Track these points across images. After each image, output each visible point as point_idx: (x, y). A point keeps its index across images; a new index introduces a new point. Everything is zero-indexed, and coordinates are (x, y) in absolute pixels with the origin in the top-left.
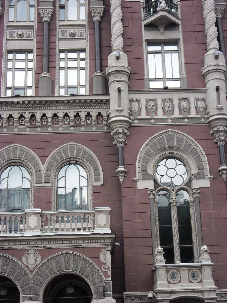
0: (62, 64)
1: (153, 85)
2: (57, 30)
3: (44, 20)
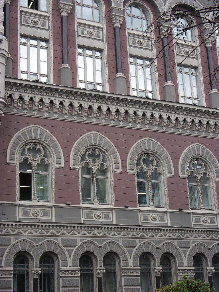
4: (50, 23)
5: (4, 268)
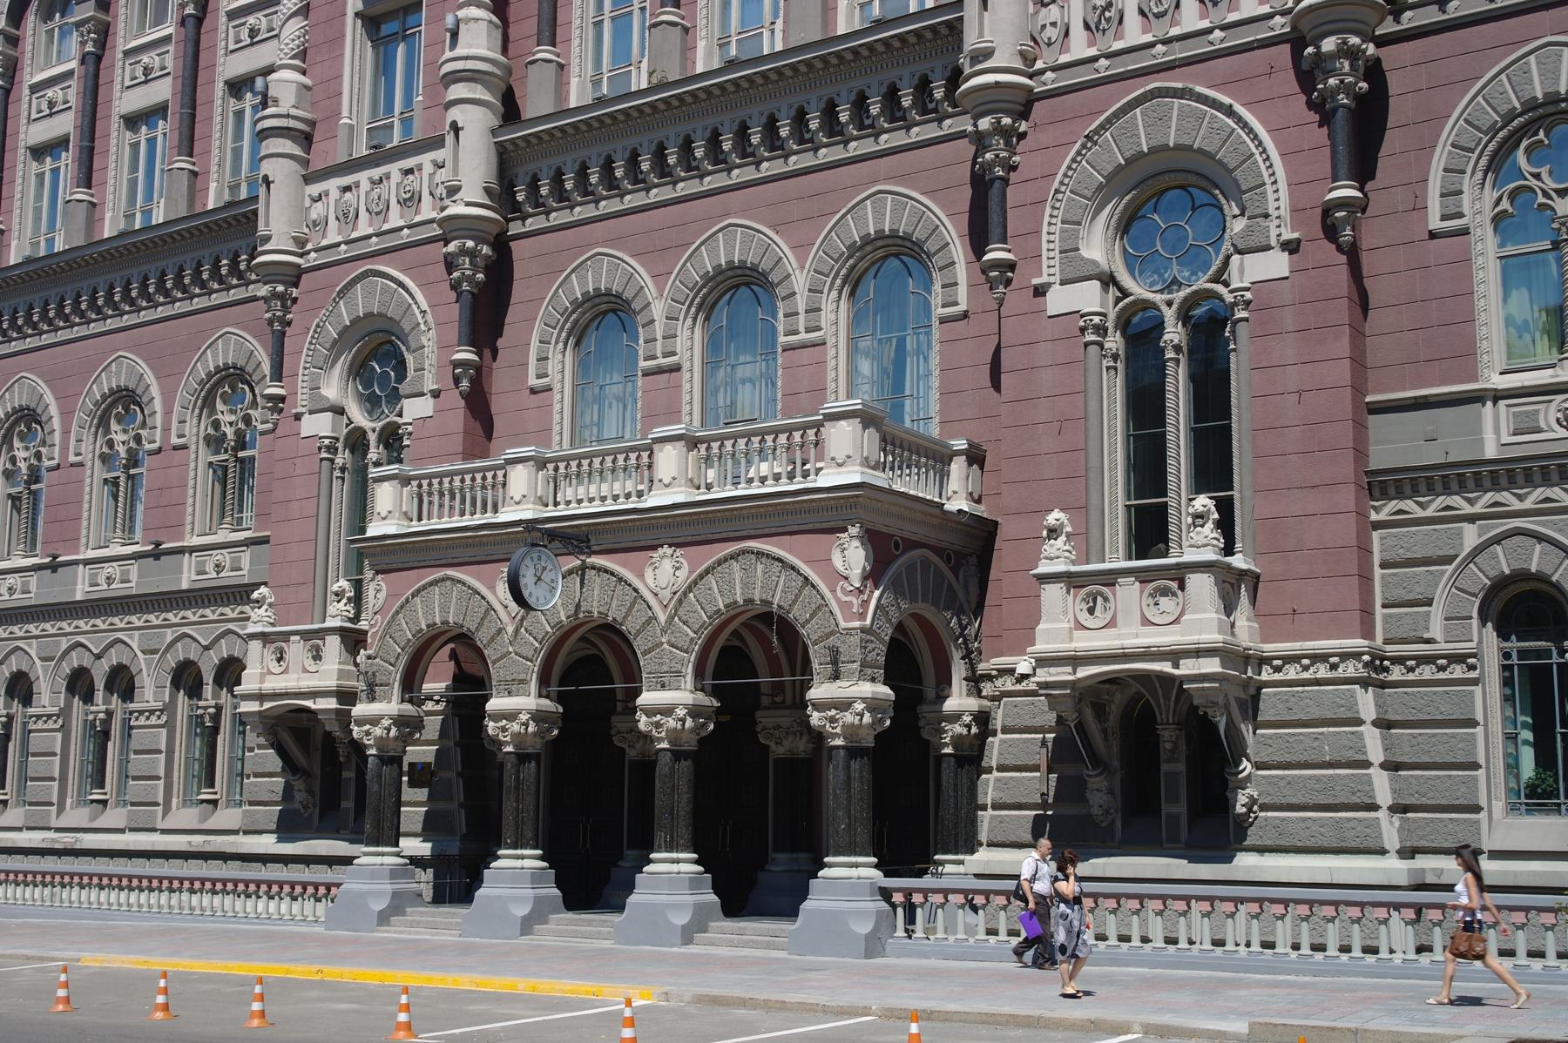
5: (1443, 647)
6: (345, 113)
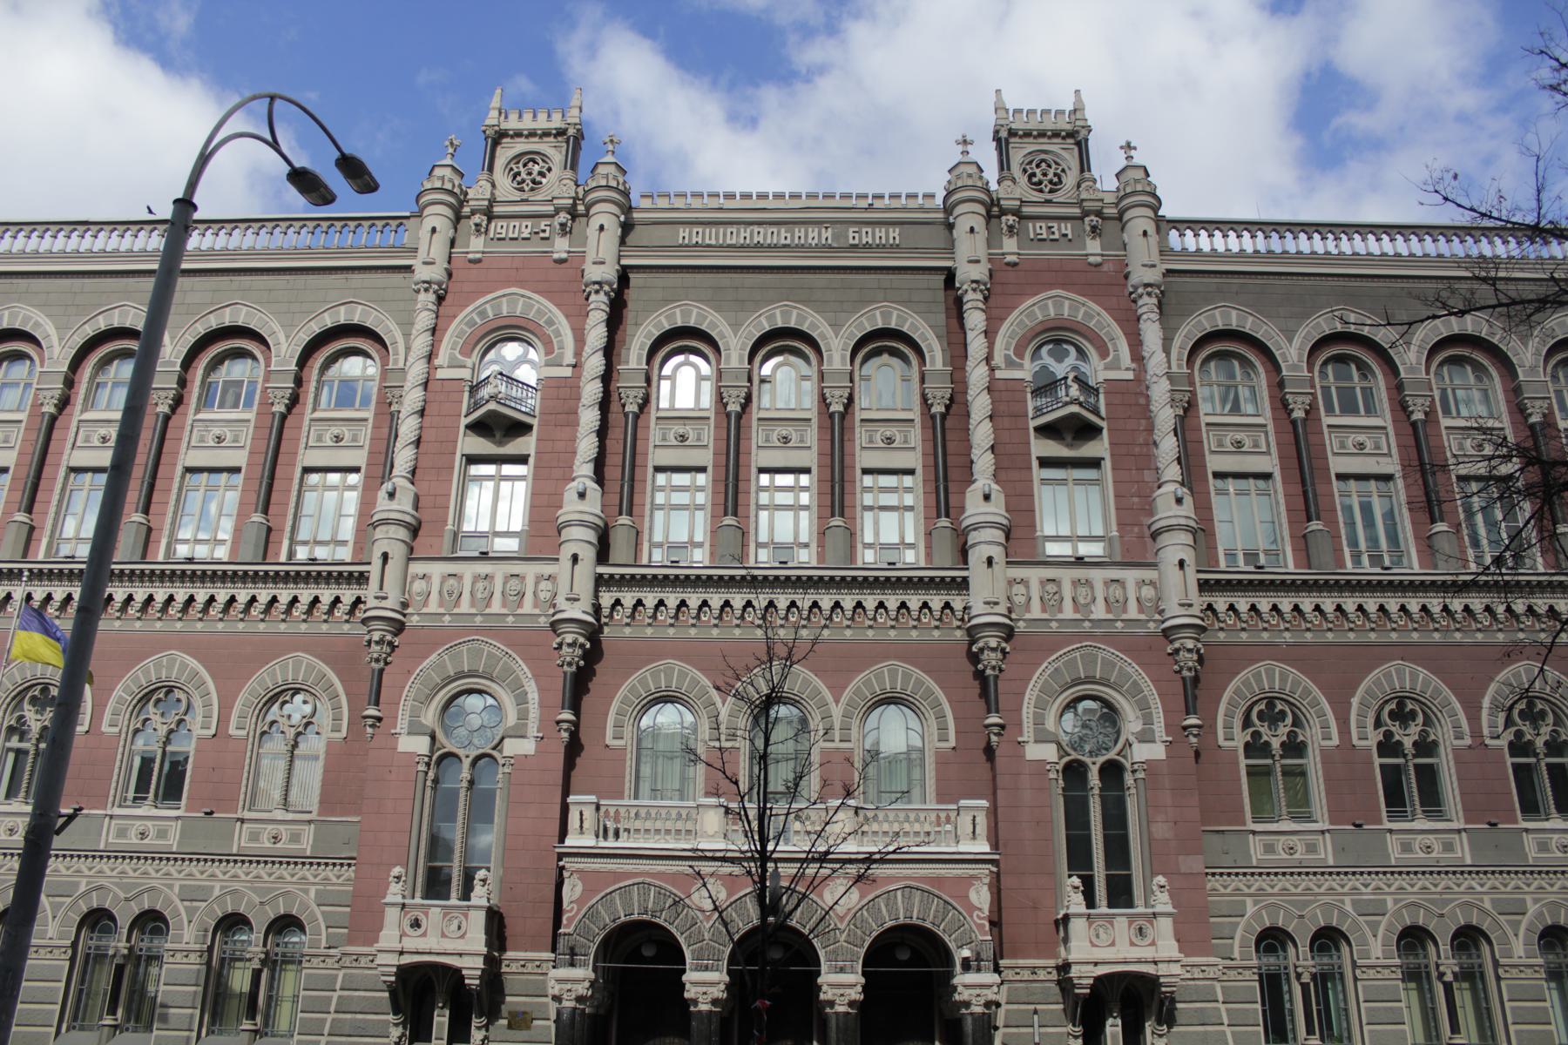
0: (868, 499)
1: (1053, 549)
2: (857, 430)
3: (832, 409)
4: (1271, 439)
6: (450, 521)
